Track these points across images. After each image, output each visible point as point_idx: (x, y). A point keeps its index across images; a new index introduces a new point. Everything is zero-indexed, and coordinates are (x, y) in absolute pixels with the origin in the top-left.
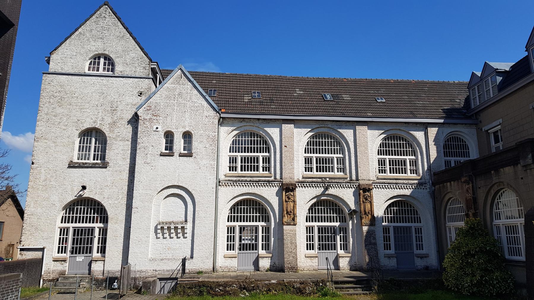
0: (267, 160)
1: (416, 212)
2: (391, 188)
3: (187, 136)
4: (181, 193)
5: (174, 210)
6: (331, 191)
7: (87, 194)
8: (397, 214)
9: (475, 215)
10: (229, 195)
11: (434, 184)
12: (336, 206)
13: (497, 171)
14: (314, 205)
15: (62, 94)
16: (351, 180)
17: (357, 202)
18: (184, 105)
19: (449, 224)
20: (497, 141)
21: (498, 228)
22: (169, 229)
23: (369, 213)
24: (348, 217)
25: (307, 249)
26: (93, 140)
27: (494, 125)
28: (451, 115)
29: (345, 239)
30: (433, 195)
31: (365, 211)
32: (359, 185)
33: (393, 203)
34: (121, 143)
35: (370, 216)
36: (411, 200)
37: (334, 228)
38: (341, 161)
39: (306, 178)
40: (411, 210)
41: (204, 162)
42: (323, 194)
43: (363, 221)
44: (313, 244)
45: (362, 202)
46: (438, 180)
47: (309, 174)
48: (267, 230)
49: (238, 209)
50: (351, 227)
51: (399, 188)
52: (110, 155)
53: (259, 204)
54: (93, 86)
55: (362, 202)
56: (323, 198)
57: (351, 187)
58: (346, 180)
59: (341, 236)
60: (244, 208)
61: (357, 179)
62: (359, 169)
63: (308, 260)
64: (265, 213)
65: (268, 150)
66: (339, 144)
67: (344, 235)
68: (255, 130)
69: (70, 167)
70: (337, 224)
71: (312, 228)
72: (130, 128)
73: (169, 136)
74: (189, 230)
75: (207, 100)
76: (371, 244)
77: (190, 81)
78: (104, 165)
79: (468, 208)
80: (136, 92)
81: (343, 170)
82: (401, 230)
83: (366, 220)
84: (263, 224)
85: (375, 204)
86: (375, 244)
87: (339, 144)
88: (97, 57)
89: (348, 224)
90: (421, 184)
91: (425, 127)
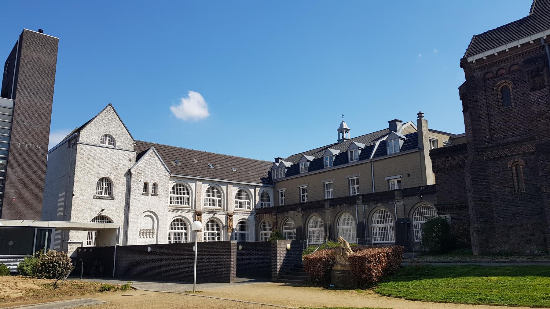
0: (188, 199)
1: (247, 226)
3: (155, 185)
4: (152, 215)
5: (147, 224)
6: (216, 216)
7: (104, 213)
9: (276, 228)
10: (172, 216)
11: (256, 214)
13: (287, 212)
15: (89, 156)
17: (227, 221)
18: (153, 168)
19: (261, 232)
20: (282, 196)
21: (285, 234)
22: (146, 232)
24: (221, 228)
26: (104, 184)
27: (282, 190)
28: (264, 180)
30: (256, 219)
34: (121, 187)
38: (220, 201)
41: (163, 199)
42: (212, 217)
46: (259, 212)
47: (206, 207)
52: (115, 193)
54: (105, 154)
65: (188, 194)
66: (220, 193)
68: (183, 183)
69: (94, 198)
70: (216, 232)
72: (125, 179)
73: (146, 184)
74: (155, 234)
75: (165, 167)
77: (157, 156)
78: (113, 198)
79: (274, 225)
80: (128, 159)
81: (220, 205)
84: (185, 231)
87: (219, 192)
88: (106, 136)
90: (251, 214)
91: (255, 187)
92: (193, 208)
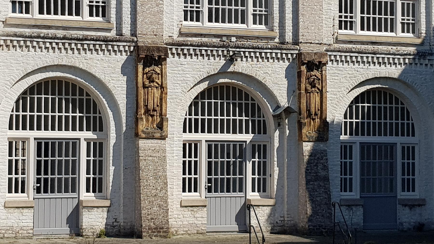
1: (405, 114)
2: (363, 62)
8: (369, 118)
12: (247, 98)
14: (202, 95)
16: (283, 42)
17: (294, 90)
23: (316, 114)
24: (271, 123)
25: (184, 191)
29: (262, 169)
31: (308, 110)
32: (300, 55)
33: (362, 94)
35: (318, 120)
36: (400, 89)
37: (241, 146)
39: (187, 35)
40: (397, 109)
42: (223, 72)
43: (304, 131)
44: (196, 179)
45: (303, 92)
48: (98, 148)
49: (32, 100)
50: (276, 144)
51: (379, 63)
53: (81, 90)
55: (303, 92)
56: (221, 81)
57: (283, 59)
58: (271, 44)
59: (254, 163)
60: (46, 100)
61: (296, 42)
62: (301, 20)
63: (187, 212)
64: (95, 112)
67: (262, 160)
70: (248, 137)
71: (196, 145)
76: (317, 178)
82: (380, 151)
83: (309, 131)
84: (90, 135)
85: (329, 95)
86: (326, 179)
89: (271, 139)
92: (126, 30)
